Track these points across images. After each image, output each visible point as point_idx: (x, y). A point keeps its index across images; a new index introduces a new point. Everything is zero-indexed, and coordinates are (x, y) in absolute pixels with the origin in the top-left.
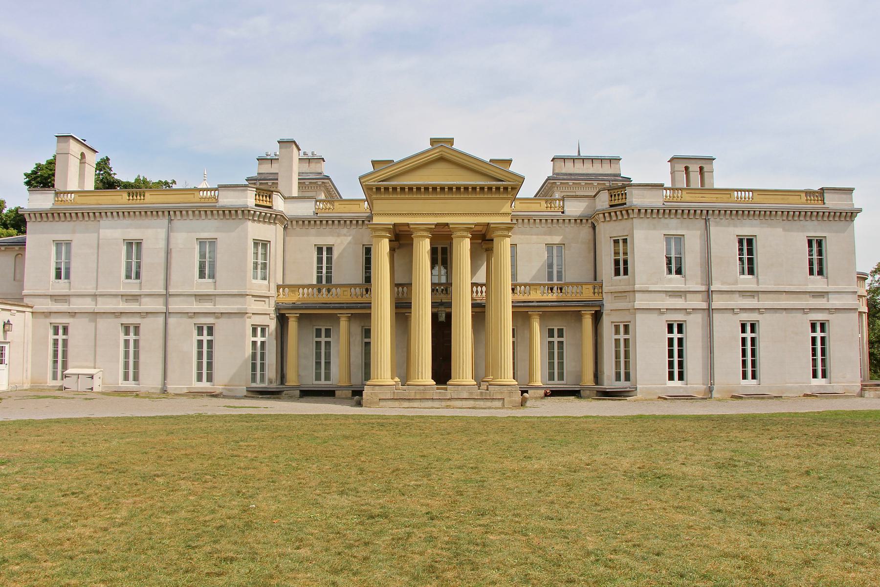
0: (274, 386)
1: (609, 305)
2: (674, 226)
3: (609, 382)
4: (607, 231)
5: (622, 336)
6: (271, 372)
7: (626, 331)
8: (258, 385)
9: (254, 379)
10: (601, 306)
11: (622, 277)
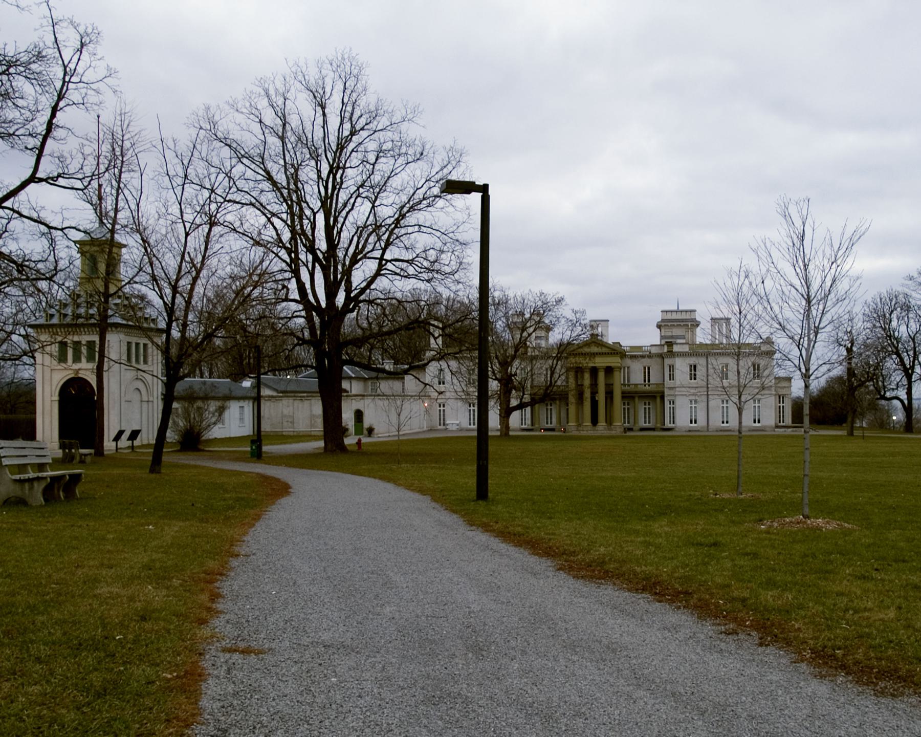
0: (530, 427)
1: (667, 392)
2: (692, 360)
3: (668, 424)
4: (668, 361)
5: (672, 406)
6: (529, 422)
7: (673, 404)
8: (524, 426)
9: (522, 424)
10: (663, 392)
11: (672, 381)
